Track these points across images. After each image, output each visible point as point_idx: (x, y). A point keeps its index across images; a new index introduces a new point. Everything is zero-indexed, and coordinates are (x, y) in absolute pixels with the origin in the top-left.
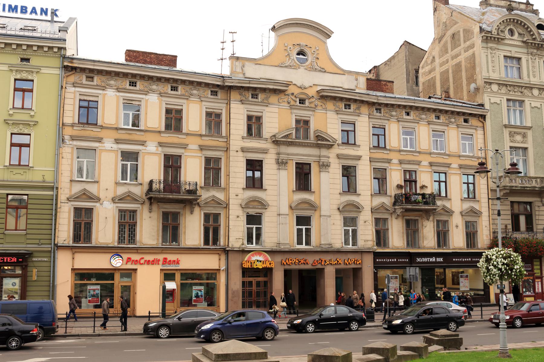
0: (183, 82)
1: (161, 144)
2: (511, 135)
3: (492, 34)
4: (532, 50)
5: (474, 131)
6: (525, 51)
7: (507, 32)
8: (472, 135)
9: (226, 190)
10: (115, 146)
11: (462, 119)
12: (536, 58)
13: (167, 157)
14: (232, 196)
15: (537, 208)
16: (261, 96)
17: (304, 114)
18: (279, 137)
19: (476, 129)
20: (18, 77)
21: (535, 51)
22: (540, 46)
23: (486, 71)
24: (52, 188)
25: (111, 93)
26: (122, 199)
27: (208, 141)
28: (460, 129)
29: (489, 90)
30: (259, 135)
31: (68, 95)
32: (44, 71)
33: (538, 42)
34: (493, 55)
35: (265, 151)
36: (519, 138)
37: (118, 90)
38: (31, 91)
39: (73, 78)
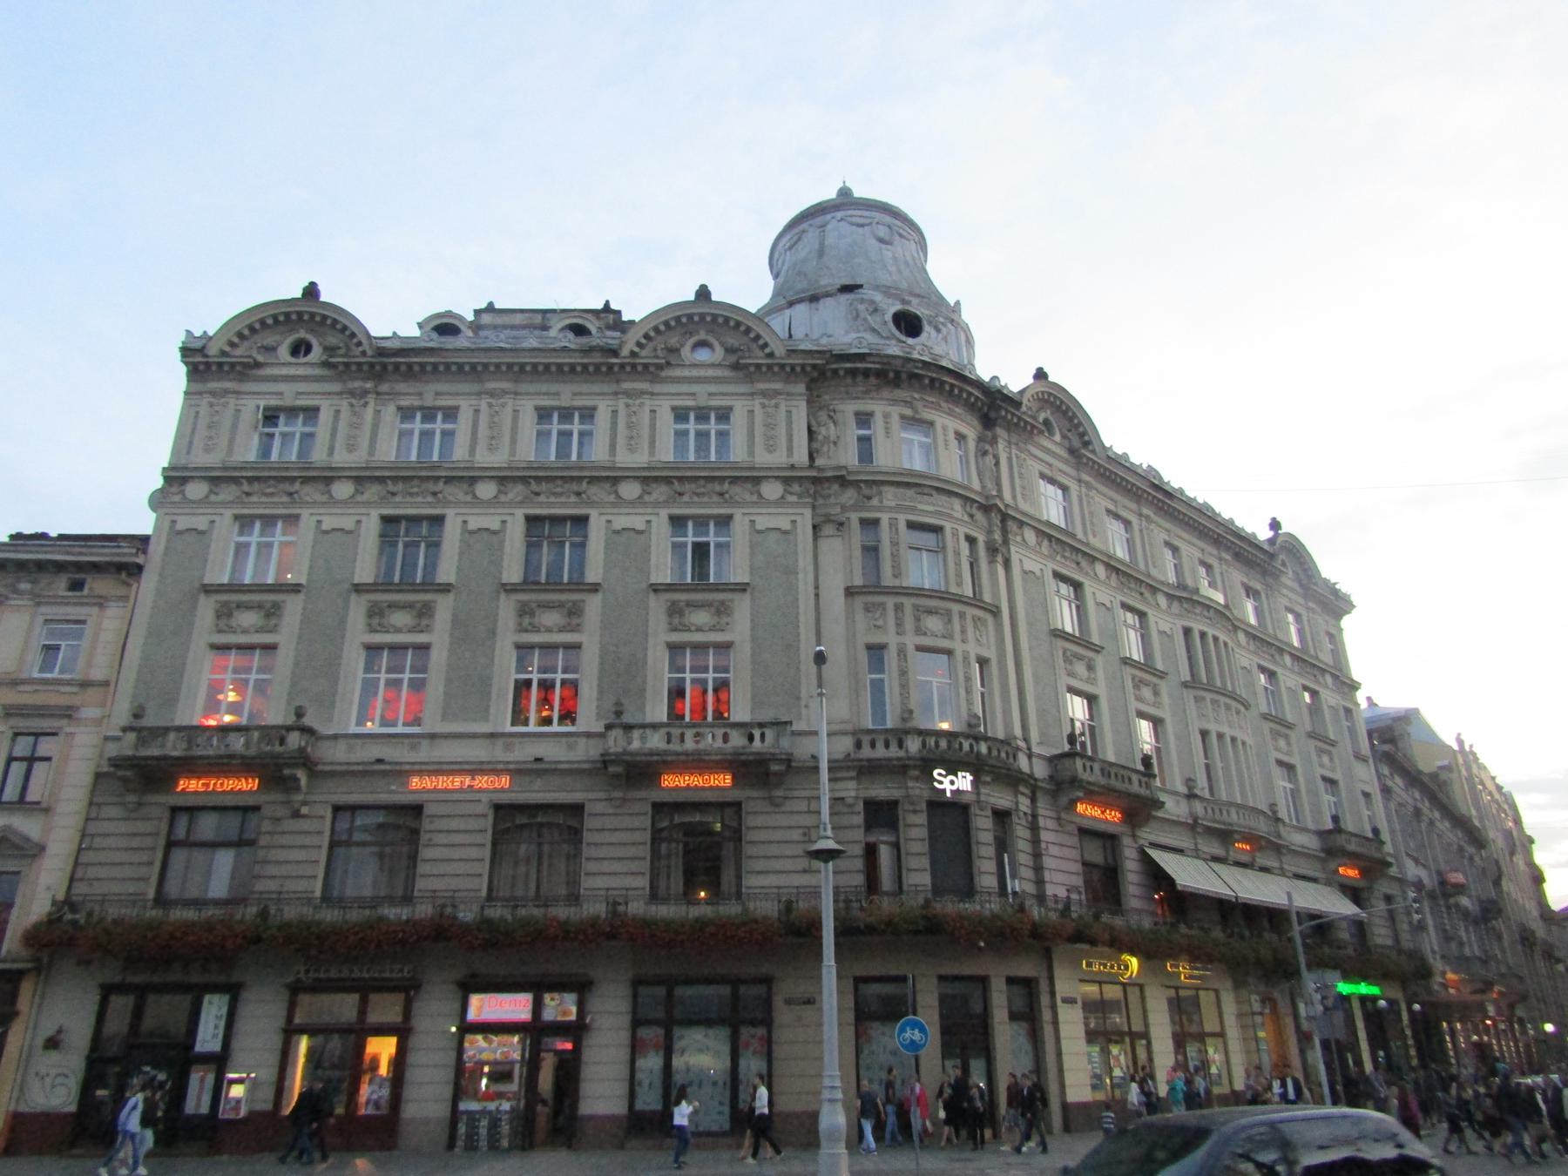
2: (224, 613)
3: (206, 356)
4: (357, 384)
5: (95, 610)
6: (335, 387)
7: (284, 353)
8: (83, 622)
11: (61, 585)
12: (366, 403)
15: (266, 826)
19: (101, 605)
21: (369, 385)
22: (378, 368)
23: (185, 451)
28: (43, 609)
29: (177, 498)
33: (370, 360)
34: (217, 408)
36: (248, 619)
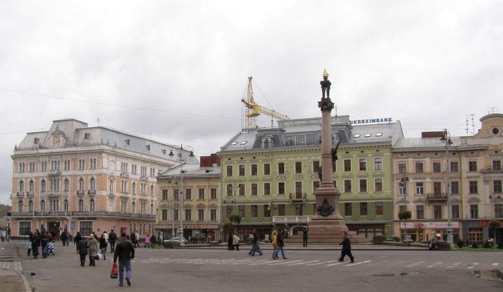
0: (439, 151)
1: (432, 178)
9: (461, 195)
10: (414, 181)
13: (435, 183)
14: (463, 197)
16: (475, 153)
17: (497, 158)
18: (483, 171)
20: (376, 158)
24: (390, 199)
25: (410, 159)
26: (417, 201)
27: (453, 175)
30: (475, 170)
31: (394, 163)
32: (385, 154)
35: (478, 177)
37: (413, 158)
38: (381, 162)
39: (395, 156)
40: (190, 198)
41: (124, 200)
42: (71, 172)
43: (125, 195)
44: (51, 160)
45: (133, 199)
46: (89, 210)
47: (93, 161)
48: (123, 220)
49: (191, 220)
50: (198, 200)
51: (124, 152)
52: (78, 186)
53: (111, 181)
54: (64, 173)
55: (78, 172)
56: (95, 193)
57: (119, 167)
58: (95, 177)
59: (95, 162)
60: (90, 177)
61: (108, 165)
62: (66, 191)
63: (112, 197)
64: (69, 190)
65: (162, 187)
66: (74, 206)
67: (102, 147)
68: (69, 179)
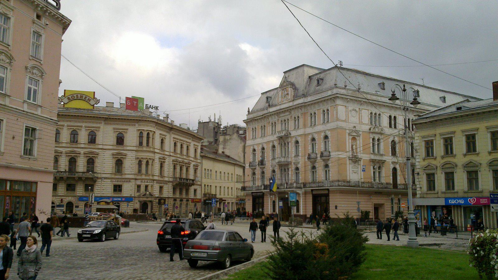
40: (475, 150)
41: (378, 165)
42: (301, 132)
43: (378, 158)
44: (280, 119)
45: (393, 163)
46: (324, 178)
47: (326, 112)
48: (378, 193)
49: (480, 190)
50: (490, 153)
51: (374, 98)
52: (310, 148)
53: (354, 139)
54: (293, 133)
55: (309, 130)
56: (330, 156)
57: (366, 118)
58: (329, 134)
59: (328, 113)
60: (323, 135)
61: (347, 116)
62: (297, 155)
63: (355, 160)
64: (300, 154)
65: (423, 137)
66: (305, 176)
67: (335, 91)
68: (299, 139)
